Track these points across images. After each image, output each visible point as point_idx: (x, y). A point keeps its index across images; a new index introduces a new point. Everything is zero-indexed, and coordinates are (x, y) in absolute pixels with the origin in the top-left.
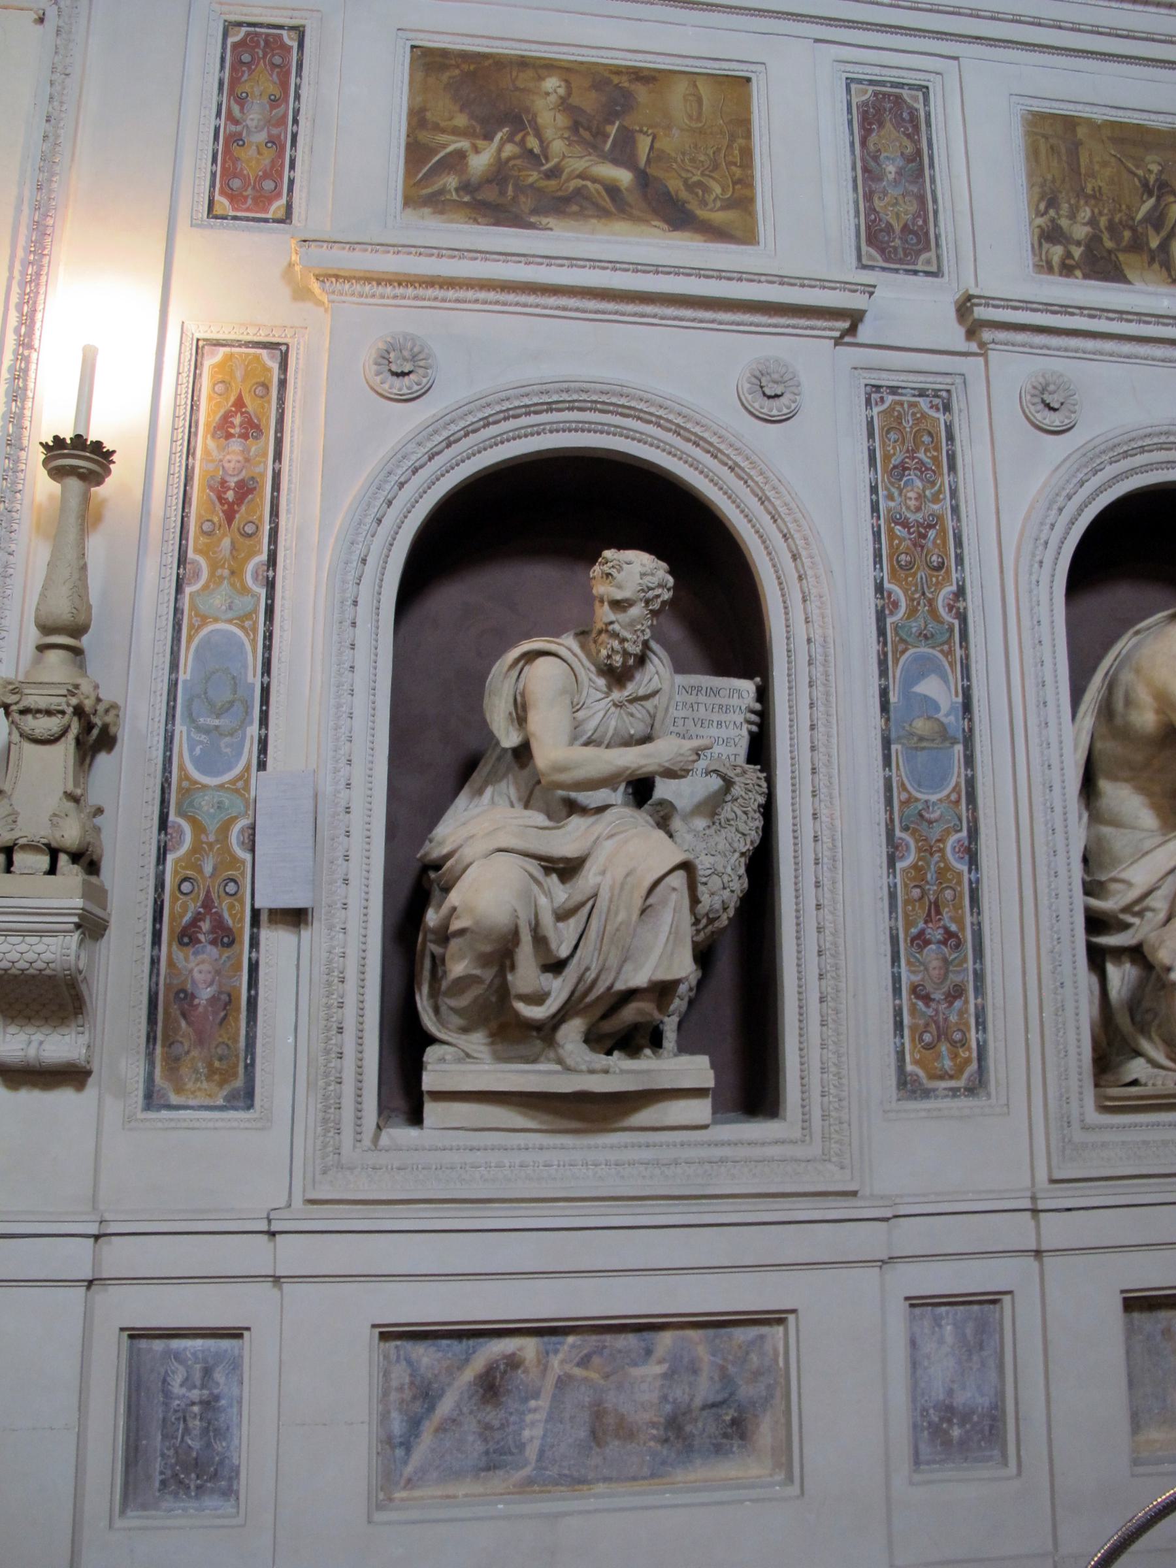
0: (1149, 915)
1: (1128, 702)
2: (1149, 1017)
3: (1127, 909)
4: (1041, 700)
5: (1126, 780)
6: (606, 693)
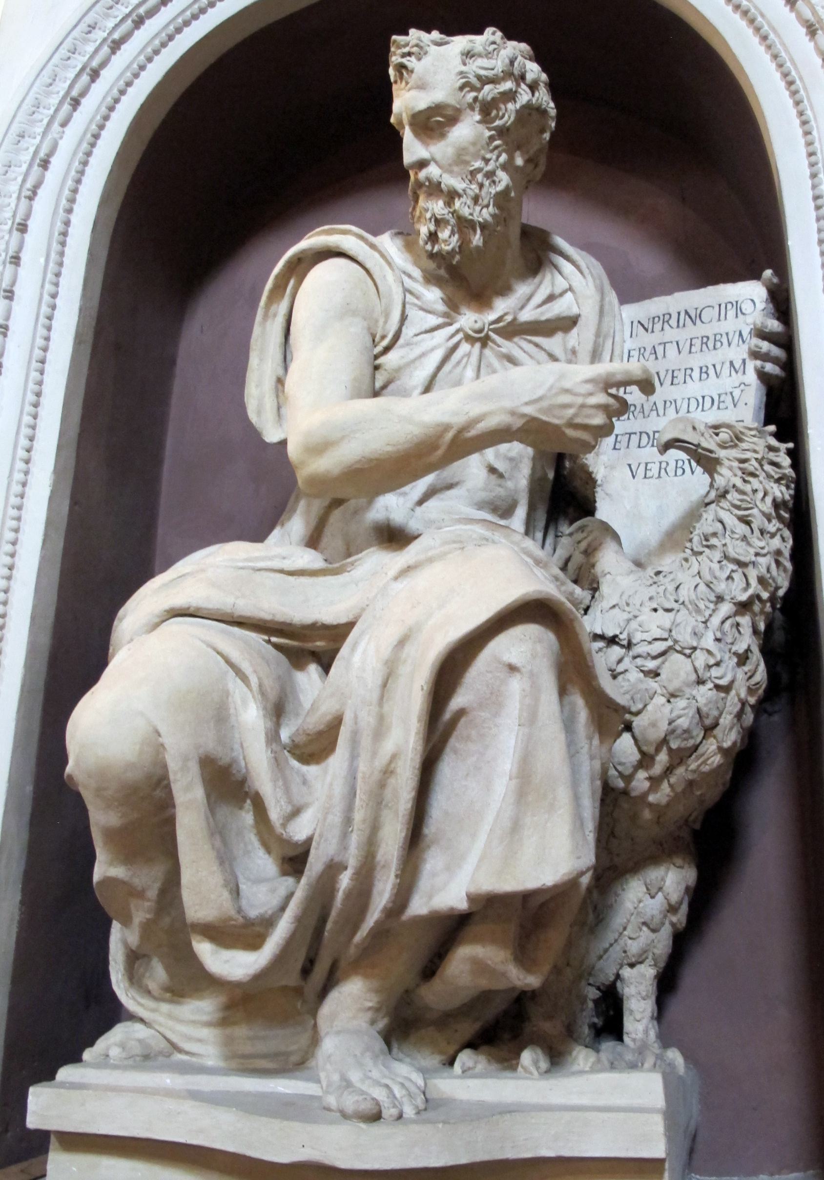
6: (445, 315)
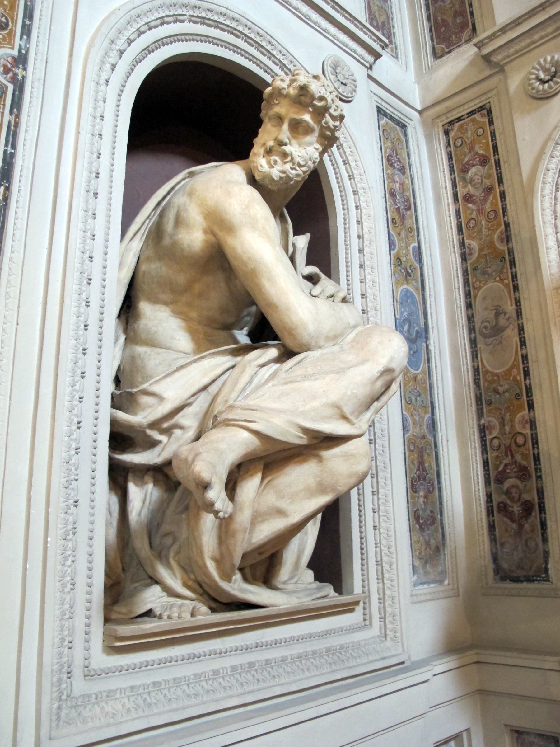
0: (177, 432)
1: (178, 222)
2: (168, 541)
3: (155, 425)
5: (166, 304)
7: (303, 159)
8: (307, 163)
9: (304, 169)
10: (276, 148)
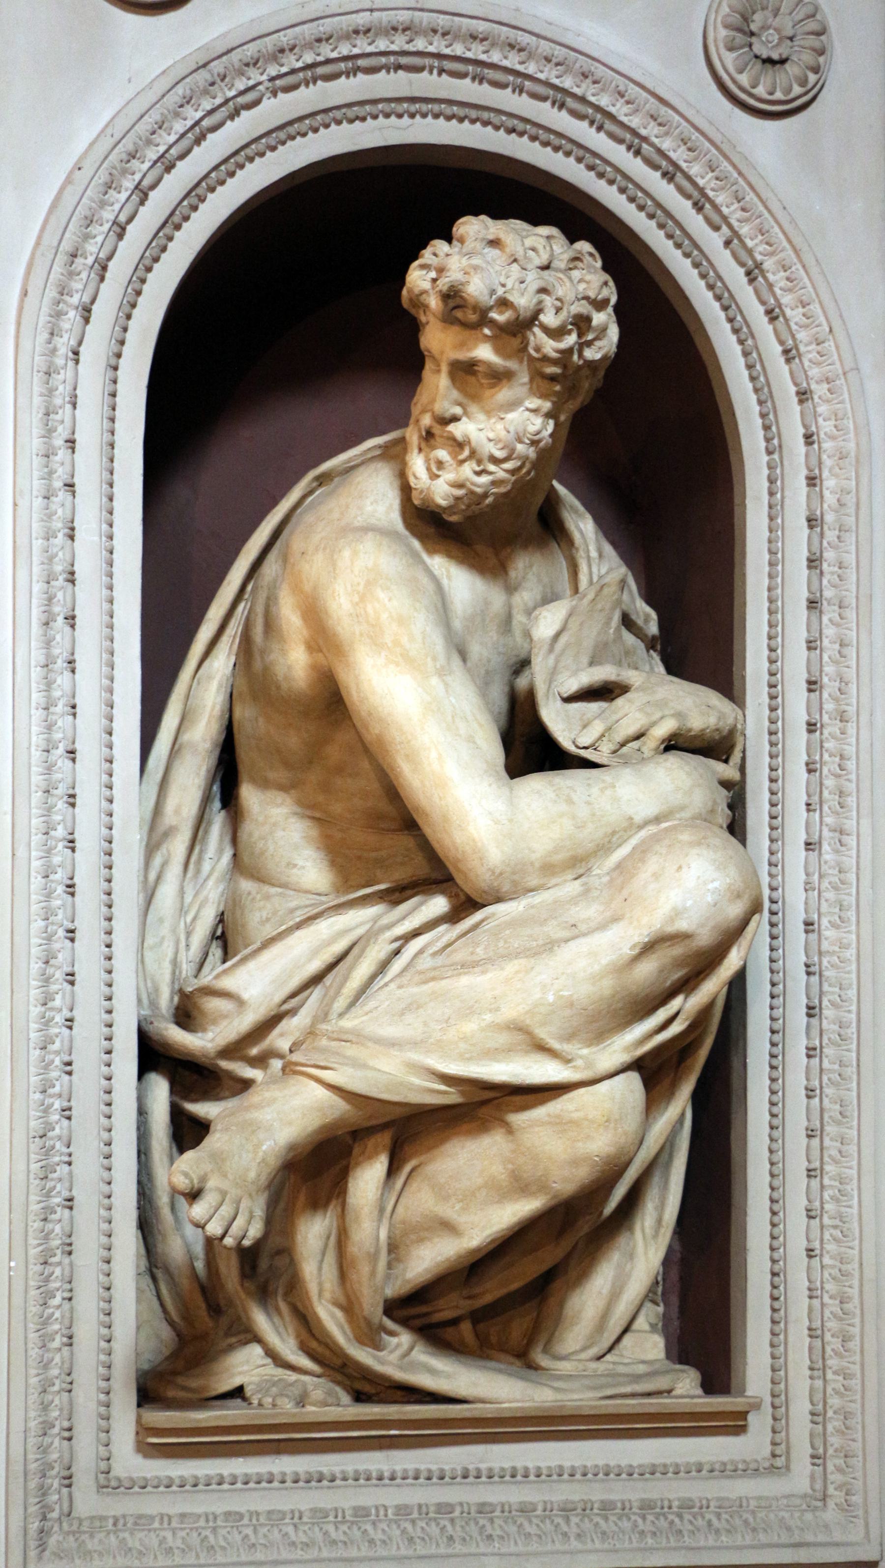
4: (60, 610)
7: (500, 446)
8: (513, 450)
9: (509, 465)
10: (437, 430)
